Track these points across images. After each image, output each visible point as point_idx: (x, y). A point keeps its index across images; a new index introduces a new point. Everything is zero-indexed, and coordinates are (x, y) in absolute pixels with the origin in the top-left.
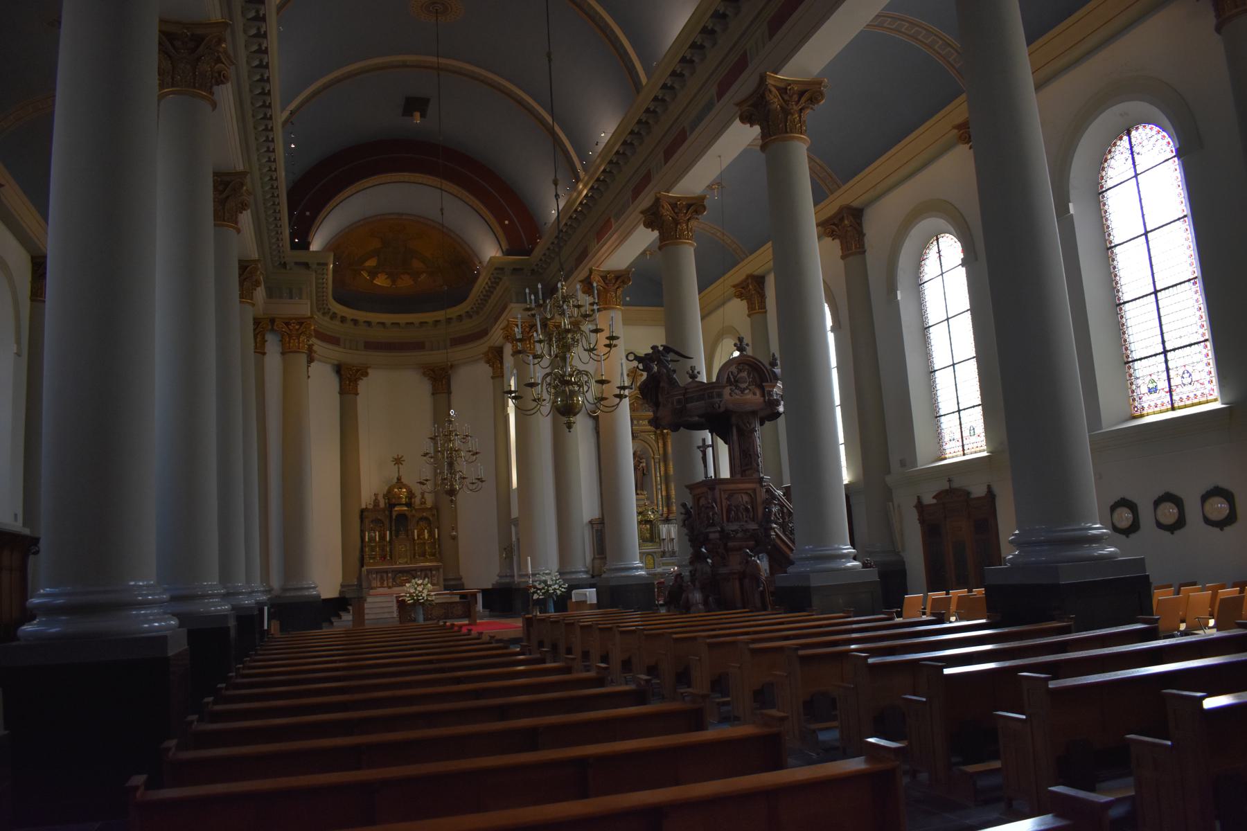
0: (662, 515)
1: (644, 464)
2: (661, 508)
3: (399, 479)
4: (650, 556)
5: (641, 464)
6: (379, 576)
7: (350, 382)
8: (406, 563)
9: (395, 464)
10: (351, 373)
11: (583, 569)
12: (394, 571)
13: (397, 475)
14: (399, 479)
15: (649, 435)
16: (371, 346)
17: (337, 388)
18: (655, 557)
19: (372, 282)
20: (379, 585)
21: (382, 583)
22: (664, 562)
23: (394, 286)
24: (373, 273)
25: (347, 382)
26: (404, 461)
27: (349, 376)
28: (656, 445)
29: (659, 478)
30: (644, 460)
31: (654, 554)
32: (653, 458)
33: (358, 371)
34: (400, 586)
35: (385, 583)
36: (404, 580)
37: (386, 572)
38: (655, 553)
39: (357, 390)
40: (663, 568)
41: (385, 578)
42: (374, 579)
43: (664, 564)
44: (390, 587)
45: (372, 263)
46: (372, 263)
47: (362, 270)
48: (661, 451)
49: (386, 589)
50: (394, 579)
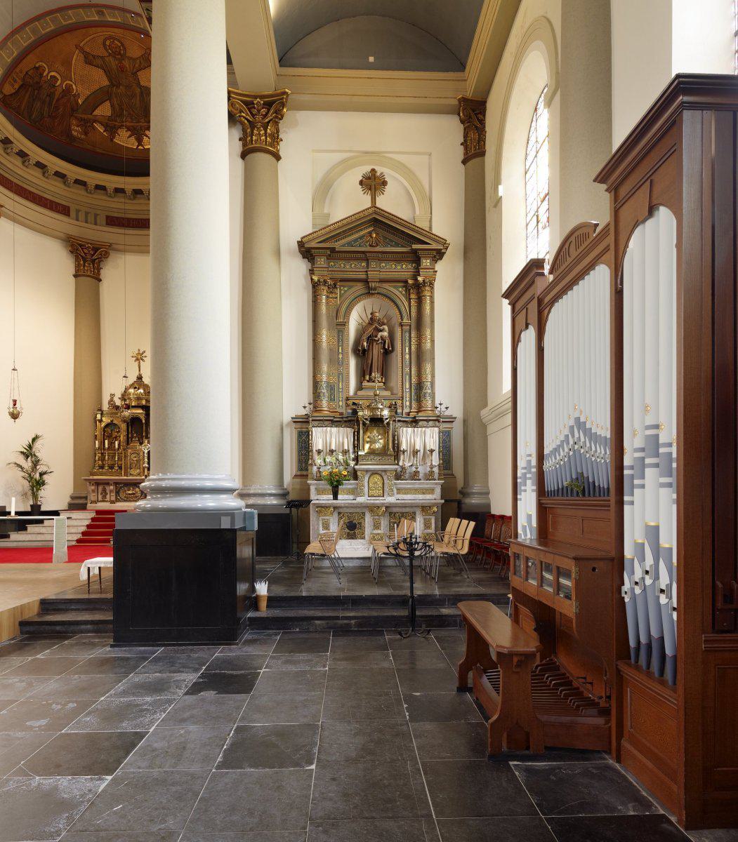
0: (408, 414)
1: (385, 334)
2: (408, 403)
3: (140, 378)
4: (378, 477)
5: (380, 334)
6: (100, 488)
7: (85, 261)
8: (139, 474)
9: (135, 361)
10: (86, 251)
11: (274, 492)
12: (116, 483)
13: (137, 373)
14: (140, 378)
15: (395, 287)
16: (112, 221)
17: (72, 271)
18: (385, 478)
19: (112, 140)
20: (100, 498)
21: (104, 497)
22: (399, 486)
23: (140, 147)
24: (112, 129)
25: (82, 262)
26: (146, 357)
27: (83, 254)
28: (406, 304)
29: (407, 357)
30: (386, 327)
31: (383, 474)
32: (401, 325)
33: (95, 250)
34: (125, 501)
35: (108, 496)
36: (130, 494)
37: (107, 483)
38: (385, 471)
39: (99, 274)
40: (400, 496)
41: (108, 492)
42: (93, 491)
43: (399, 491)
44: (112, 502)
45: (104, 110)
46: (104, 110)
47: (95, 121)
48: (414, 314)
49: (108, 504)
50: (117, 493)
